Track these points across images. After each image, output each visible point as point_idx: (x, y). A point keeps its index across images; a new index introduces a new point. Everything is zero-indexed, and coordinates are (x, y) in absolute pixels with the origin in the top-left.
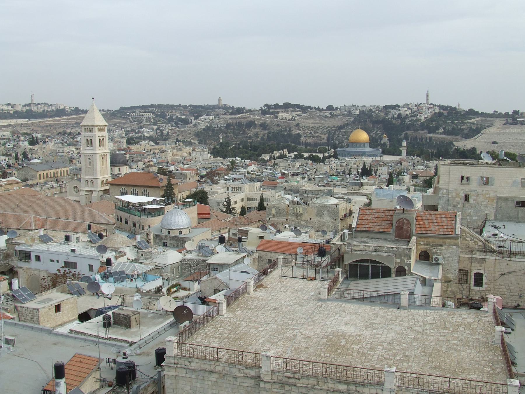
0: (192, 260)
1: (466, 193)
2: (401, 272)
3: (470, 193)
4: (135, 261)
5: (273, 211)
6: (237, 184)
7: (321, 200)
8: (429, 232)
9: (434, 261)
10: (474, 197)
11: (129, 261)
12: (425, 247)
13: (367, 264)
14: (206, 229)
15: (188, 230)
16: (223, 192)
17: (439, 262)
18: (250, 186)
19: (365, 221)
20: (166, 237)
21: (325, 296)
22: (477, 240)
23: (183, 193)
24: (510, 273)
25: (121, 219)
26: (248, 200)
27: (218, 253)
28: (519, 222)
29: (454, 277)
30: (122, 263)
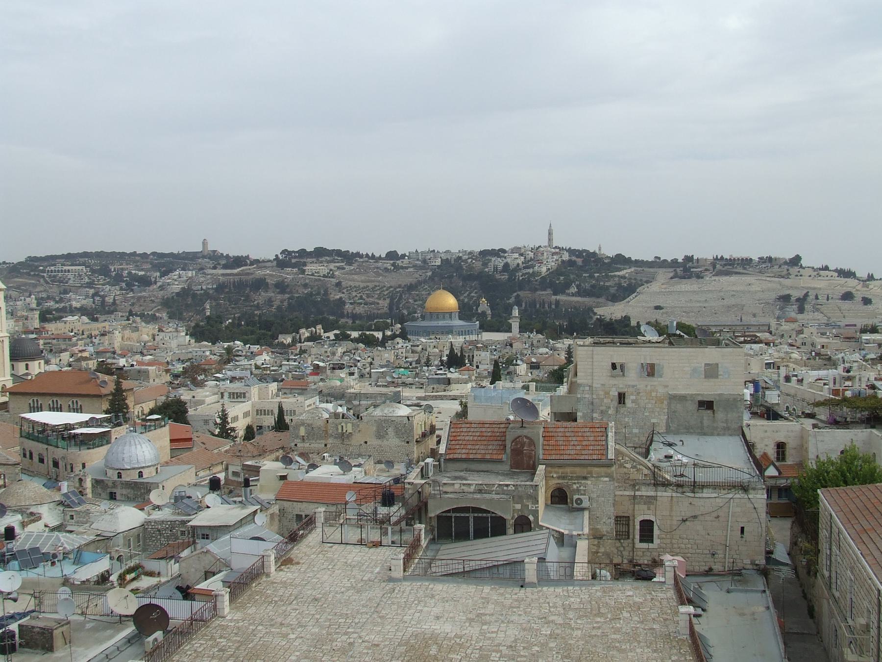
0: (163, 521)
1: (621, 391)
2: (524, 525)
3: (626, 390)
4: (60, 528)
5: (302, 431)
6: (237, 387)
7: (382, 410)
8: (566, 457)
11: (47, 529)
12: (560, 481)
13: (467, 515)
14: (187, 467)
15: (153, 469)
16: (213, 401)
17: (584, 505)
18: (260, 389)
19: (460, 442)
20: (114, 483)
21: (398, 573)
22: (641, 467)
23: (143, 405)
24: (695, 517)
25: (31, 454)
27: (208, 507)
28: (705, 434)
29: (609, 530)
30: (35, 534)
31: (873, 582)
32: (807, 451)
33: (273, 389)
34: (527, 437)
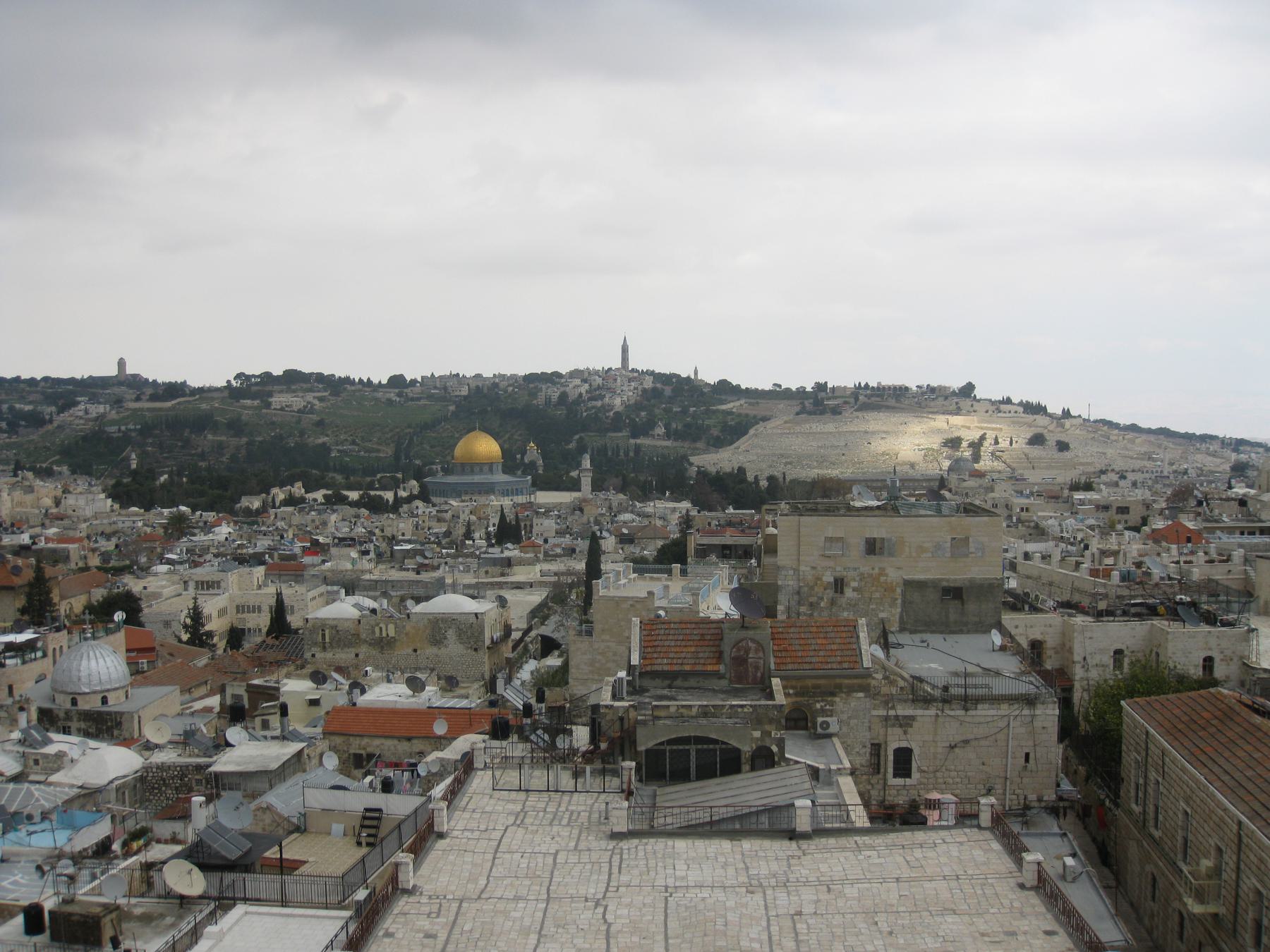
1: (838, 574)
2: (765, 759)
8: (806, 666)
9: (819, 730)
10: (854, 584)
13: (687, 747)
14: (170, 688)
15: (121, 693)
16: (173, 594)
18: (241, 576)
19: (659, 649)
20: (67, 712)
23: (73, 600)
24: (966, 742)
26: (238, 612)
31: (1225, 810)
32: (1070, 651)
33: (259, 575)
34: (753, 640)
